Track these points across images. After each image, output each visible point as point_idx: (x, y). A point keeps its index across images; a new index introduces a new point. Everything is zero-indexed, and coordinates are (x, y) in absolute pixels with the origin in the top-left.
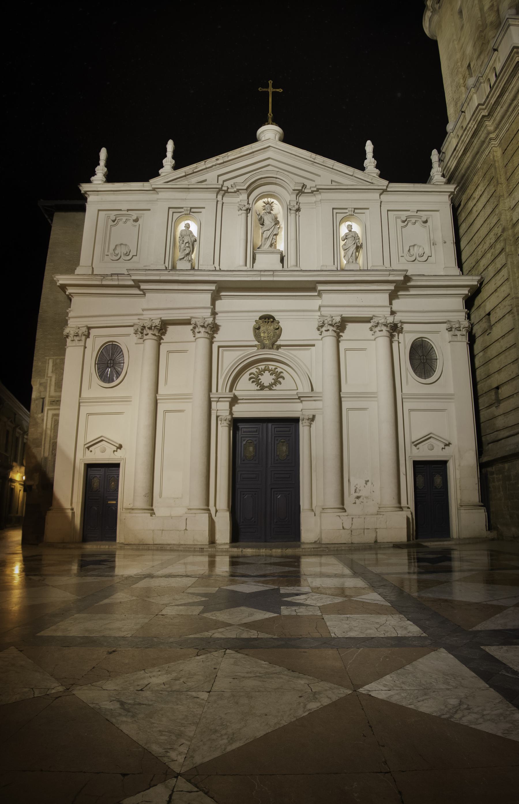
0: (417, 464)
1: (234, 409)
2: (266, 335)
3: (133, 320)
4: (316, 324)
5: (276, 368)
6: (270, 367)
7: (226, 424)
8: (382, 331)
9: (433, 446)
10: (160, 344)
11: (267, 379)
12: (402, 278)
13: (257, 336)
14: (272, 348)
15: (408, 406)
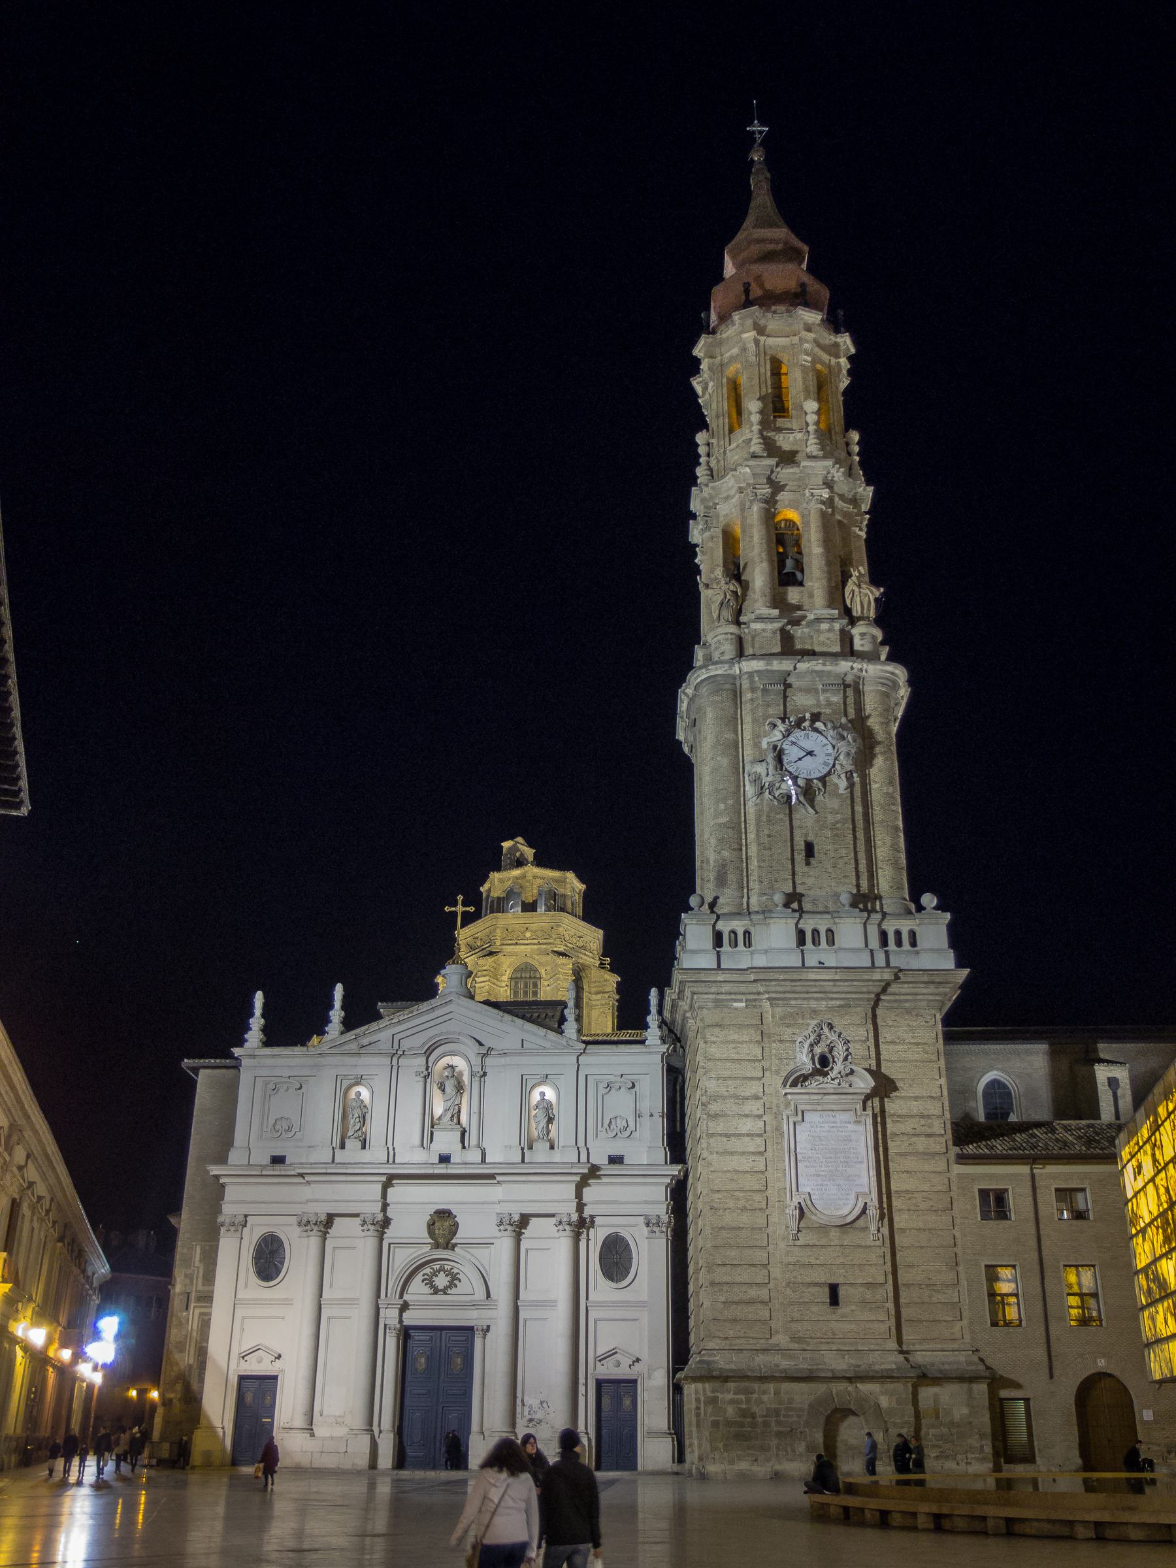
0: (599, 1383)
1: (405, 1315)
2: (441, 1231)
3: (298, 1209)
4: (494, 1220)
5: (452, 1269)
6: (446, 1267)
7: (394, 1333)
8: (565, 1230)
9: (619, 1361)
10: (325, 1239)
11: (441, 1281)
12: (586, 1171)
13: (431, 1233)
14: (446, 1247)
15: (593, 1315)
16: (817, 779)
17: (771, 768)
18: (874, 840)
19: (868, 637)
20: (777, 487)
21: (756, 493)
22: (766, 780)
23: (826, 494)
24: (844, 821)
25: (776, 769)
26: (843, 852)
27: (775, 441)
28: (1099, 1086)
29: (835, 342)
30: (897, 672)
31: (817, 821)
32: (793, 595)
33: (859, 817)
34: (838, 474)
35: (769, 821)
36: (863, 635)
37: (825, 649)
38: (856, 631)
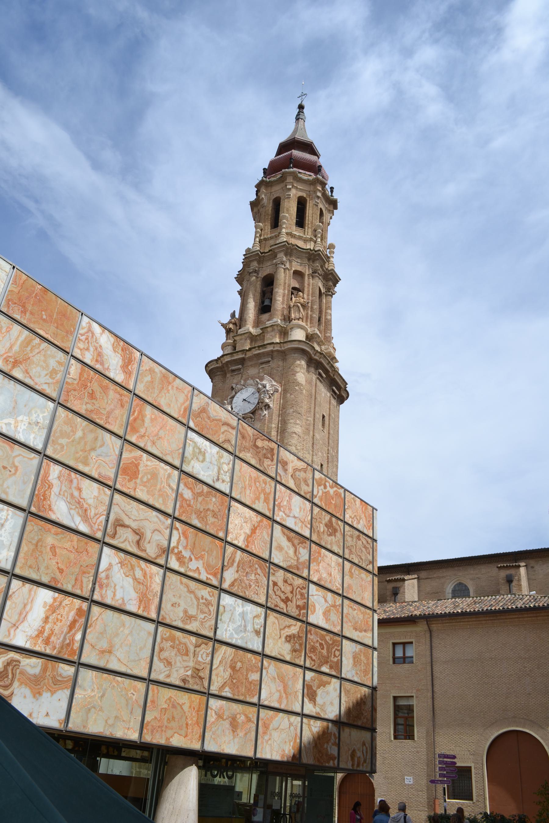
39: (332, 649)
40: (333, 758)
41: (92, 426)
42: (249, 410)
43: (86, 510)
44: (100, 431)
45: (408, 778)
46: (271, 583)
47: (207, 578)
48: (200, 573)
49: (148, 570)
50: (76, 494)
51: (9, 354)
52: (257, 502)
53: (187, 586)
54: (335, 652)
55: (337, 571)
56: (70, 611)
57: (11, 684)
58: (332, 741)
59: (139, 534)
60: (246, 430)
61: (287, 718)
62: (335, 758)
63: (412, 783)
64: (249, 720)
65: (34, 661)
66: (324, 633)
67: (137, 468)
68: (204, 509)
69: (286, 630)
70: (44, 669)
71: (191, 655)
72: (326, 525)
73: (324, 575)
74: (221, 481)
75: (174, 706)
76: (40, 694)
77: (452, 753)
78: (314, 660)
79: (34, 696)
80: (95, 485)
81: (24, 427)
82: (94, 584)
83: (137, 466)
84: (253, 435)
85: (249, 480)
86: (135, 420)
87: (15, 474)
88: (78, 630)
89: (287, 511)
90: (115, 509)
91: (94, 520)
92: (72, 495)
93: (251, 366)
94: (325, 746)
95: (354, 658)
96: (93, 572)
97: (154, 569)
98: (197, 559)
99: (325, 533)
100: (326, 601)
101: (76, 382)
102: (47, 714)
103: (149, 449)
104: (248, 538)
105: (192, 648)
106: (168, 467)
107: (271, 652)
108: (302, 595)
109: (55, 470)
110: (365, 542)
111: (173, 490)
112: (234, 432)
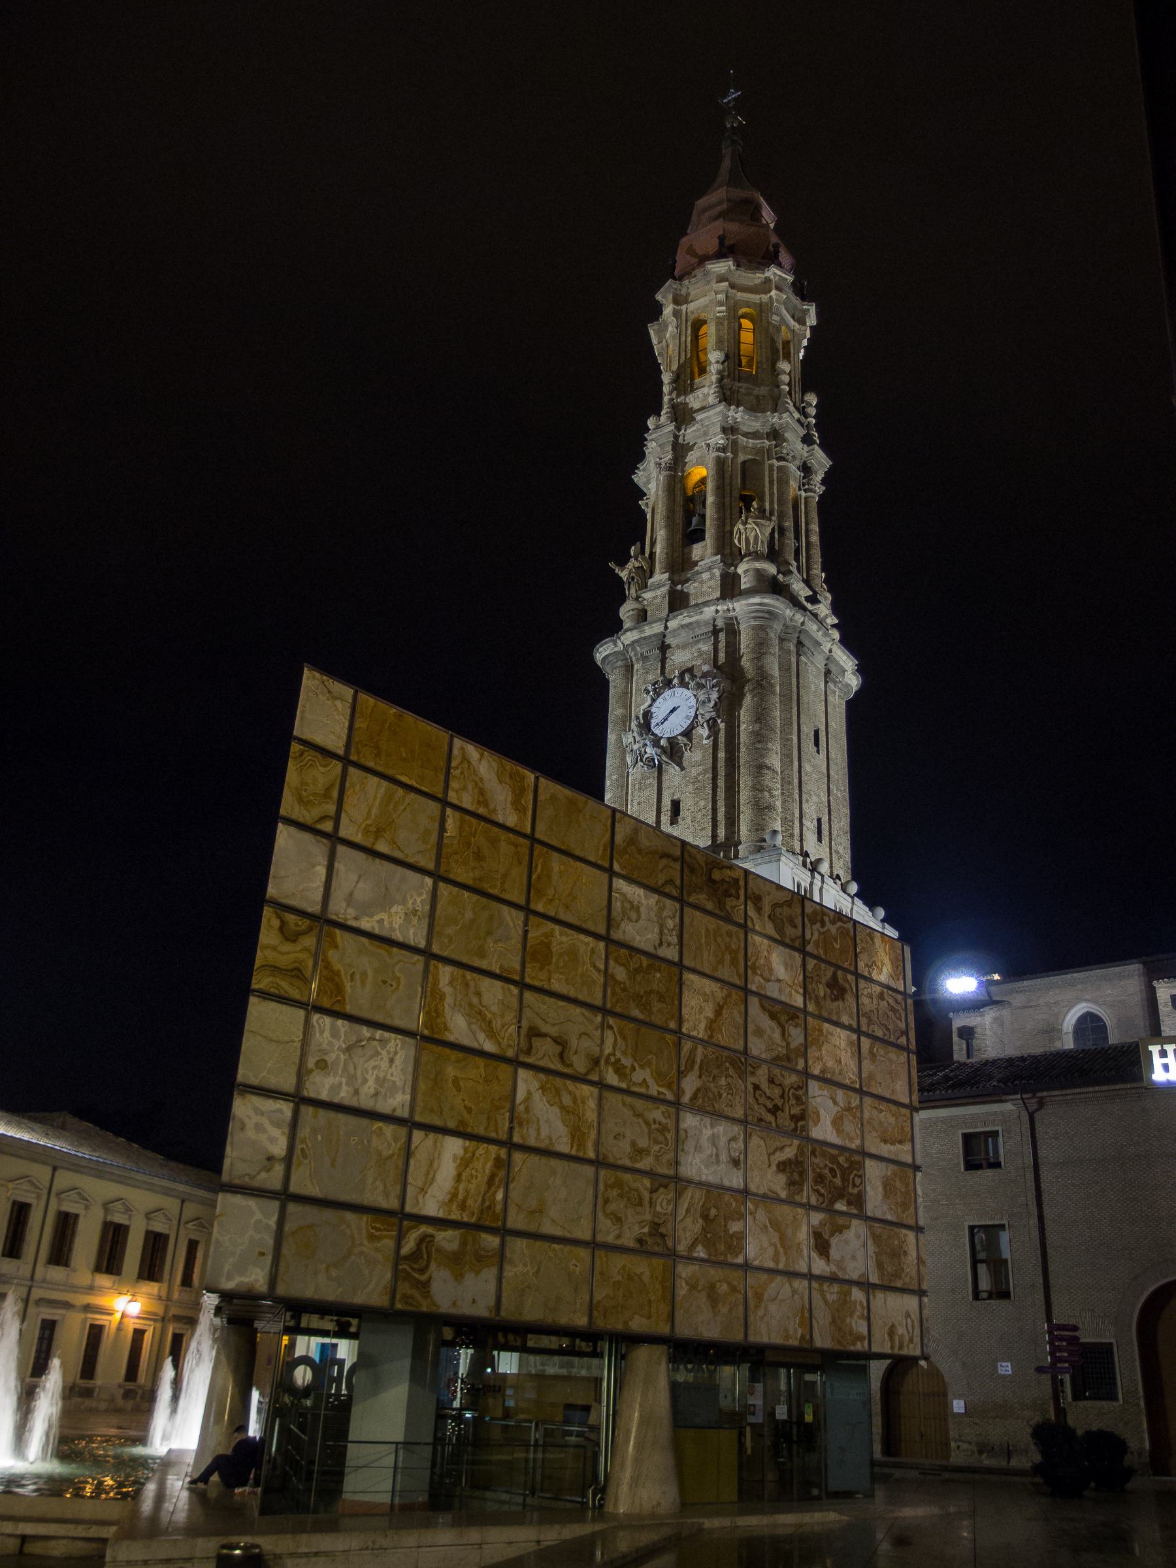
16: (680, 734)
17: (635, 734)
18: (739, 785)
19: (751, 573)
20: (680, 450)
21: (660, 464)
22: (635, 747)
23: (720, 440)
24: (705, 771)
25: (641, 735)
26: (702, 803)
27: (687, 404)
28: (1160, 1007)
29: (766, 278)
30: (766, 601)
31: (684, 777)
32: (697, 550)
33: (721, 764)
34: (738, 415)
35: (640, 788)
36: (746, 572)
37: (707, 599)
38: (740, 570)
39: (849, 1175)
40: (860, 1338)
41: (484, 900)
42: (681, 730)
43: (490, 1022)
44: (495, 905)
45: (1003, 1364)
46: (750, 1088)
47: (658, 1092)
48: (648, 1087)
49: (578, 1093)
50: (475, 1001)
51: (368, 822)
52: (720, 967)
53: (632, 1108)
54: (853, 1179)
55: (849, 1054)
56: (485, 1163)
57: (427, 1266)
58: (858, 1313)
59: (561, 1042)
60: (695, 858)
61: (787, 1285)
62: (864, 1338)
63: (1010, 1372)
64: (734, 1289)
65: (450, 1233)
66: (834, 1152)
67: (549, 948)
68: (645, 992)
69: (778, 1154)
70: (464, 1243)
71: (647, 1205)
72: (828, 985)
73: (830, 1064)
74: (665, 945)
75: (630, 1278)
76: (462, 1275)
77: (1072, 1322)
78: (822, 1195)
79: (456, 1279)
80: (498, 984)
81: (400, 921)
82: (511, 1121)
83: (548, 946)
84: (707, 864)
85: (706, 937)
86: (539, 878)
87: (397, 989)
88: (499, 1187)
89: (766, 974)
90: (527, 1013)
91: (502, 1034)
92: (471, 1005)
93: (678, 647)
94: (848, 1320)
95: (885, 1186)
96: (508, 1105)
97: (586, 1089)
98: (642, 1067)
99: (828, 998)
100: (835, 1103)
101: (455, 842)
102: (474, 1301)
103: (562, 916)
104: (711, 1025)
105: (646, 1195)
106: (590, 939)
107: (758, 1187)
108: (798, 1098)
109: (445, 973)
110: (891, 1001)
111: (599, 971)
112: (678, 866)
